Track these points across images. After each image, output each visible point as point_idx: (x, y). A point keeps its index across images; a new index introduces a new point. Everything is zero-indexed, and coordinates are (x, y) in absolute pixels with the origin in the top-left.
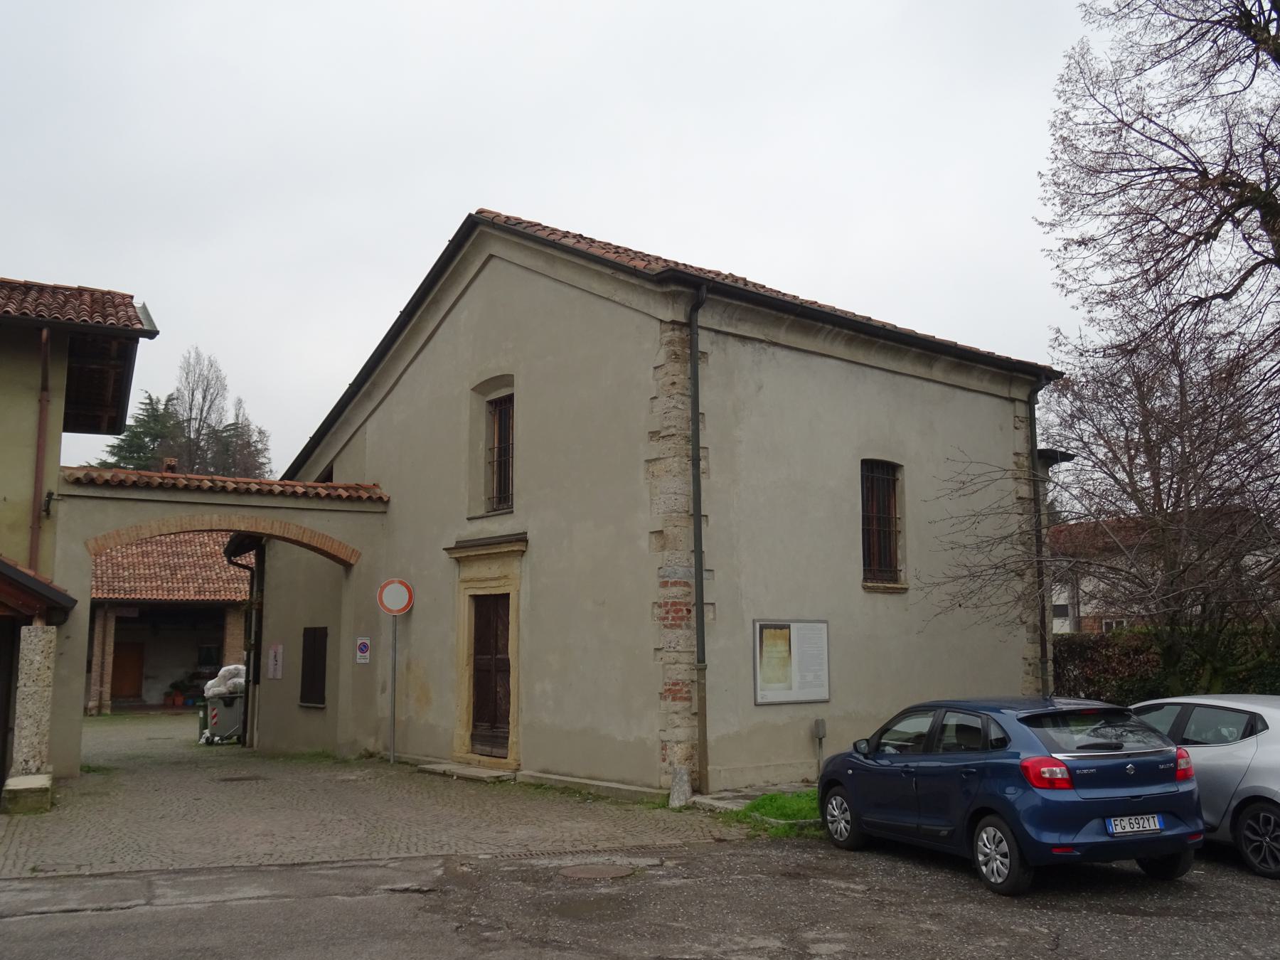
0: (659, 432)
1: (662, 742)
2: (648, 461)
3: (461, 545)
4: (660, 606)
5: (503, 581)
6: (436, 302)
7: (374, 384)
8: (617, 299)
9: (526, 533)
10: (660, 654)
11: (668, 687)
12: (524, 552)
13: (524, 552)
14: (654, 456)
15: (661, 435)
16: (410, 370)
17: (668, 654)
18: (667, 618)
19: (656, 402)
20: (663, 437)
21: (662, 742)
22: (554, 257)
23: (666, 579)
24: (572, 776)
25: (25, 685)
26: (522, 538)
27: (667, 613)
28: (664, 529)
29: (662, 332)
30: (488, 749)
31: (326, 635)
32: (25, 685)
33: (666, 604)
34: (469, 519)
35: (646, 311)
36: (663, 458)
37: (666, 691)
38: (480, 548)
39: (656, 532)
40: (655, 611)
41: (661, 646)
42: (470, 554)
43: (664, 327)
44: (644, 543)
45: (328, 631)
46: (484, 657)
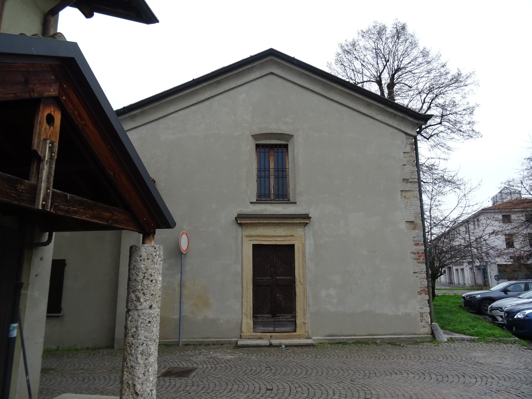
0: (409, 180)
1: (420, 313)
2: (402, 191)
3: (240, 217)
4: (414, 254)
5: (289, 238)
6: (218, 82)
7: (142, 113)
8: (378, 118)
9: (308, 215)
10: (416, 275)
11: (422, 289)
12: (307, 224)
13: (307, 224)
14: (407, 189)
15: (409, 181)
16: (181, 113)
17: (421, 275)
18: (420, 259)
19: (404, 167)
20: (411, 182)
21: (420, 313)
22: (334, 87)
23: (418, 242)
24: (355, 336)
25: (151, 307)
26: (306, 217)
27: (420, 256)
28: (415, 221)
29: (407, 139)
30: (271, 329)
31: (65, 265)
32: (151, 307)
33: (418, 253)
34: (251, 203)
35: (399, 128)
36: (411, 191)
37: (421, 291)
38: (280, 219)
39: (409, 222)
40: (412, 256)
41: (417, 271)
42: (261, 222)
43: (408, 137)
44: (403, 226)
45: (66, 262)
46: (264, 278)
